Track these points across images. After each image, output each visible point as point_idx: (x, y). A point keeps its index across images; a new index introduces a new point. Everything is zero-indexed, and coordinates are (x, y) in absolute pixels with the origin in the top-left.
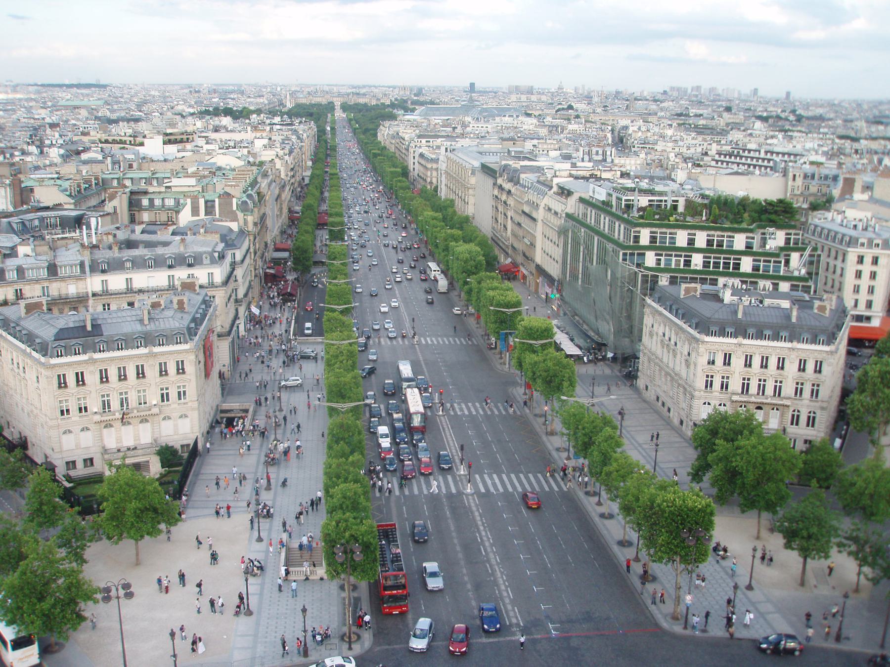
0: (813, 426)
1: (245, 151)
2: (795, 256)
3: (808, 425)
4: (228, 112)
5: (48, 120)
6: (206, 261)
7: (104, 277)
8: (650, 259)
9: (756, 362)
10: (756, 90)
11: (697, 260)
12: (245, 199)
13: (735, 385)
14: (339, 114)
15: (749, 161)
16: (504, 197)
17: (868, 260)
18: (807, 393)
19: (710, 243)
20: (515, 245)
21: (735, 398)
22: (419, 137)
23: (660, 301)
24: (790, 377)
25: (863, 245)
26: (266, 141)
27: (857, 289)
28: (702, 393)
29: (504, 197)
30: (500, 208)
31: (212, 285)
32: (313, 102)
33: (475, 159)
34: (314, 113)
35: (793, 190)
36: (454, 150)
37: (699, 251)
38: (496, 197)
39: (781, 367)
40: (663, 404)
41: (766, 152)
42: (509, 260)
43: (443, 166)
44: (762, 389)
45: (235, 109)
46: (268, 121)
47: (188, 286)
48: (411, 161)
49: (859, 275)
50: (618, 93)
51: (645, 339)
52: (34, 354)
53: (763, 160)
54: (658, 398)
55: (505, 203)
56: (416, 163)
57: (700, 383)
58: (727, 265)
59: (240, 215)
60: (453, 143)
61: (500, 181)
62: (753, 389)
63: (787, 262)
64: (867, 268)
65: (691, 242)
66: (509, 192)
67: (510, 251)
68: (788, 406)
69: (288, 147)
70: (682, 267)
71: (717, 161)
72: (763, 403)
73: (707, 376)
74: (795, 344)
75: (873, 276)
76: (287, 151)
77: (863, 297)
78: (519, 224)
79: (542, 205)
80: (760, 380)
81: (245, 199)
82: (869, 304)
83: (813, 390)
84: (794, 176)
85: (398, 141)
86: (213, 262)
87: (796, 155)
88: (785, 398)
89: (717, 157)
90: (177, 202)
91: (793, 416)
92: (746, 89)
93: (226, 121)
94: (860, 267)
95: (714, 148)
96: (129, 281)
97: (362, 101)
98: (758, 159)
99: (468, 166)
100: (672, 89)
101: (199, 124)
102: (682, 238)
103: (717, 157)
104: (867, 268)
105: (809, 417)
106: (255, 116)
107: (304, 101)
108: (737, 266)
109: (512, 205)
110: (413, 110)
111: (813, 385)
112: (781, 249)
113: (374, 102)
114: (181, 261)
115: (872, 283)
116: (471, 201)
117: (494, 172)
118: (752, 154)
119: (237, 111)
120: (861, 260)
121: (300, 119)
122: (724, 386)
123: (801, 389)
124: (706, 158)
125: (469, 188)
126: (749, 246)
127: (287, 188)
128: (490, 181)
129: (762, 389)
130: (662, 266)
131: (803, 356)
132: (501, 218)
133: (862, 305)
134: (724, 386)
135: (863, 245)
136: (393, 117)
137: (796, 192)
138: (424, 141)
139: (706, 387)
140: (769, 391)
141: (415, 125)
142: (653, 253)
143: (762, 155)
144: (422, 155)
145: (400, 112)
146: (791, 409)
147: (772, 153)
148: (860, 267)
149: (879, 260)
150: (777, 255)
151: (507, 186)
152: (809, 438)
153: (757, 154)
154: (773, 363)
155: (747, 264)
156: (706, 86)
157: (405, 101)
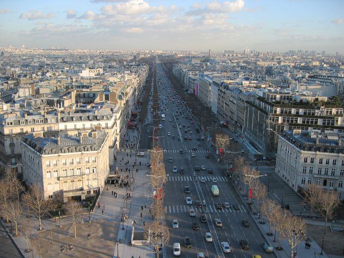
5: (45, 63)
6: (105, 118)
7: (65, 124)
12: (121, 94)
13: (315, 171)
15: (323, 80)
16: (222, 95)
19: (305, 113)
21: (315, 176)
23: (284, 136)
28: (302, 174)
31: (107, 128)
34: (148, 61)
35: (339, 92)
37: (300, 116)
38: (219, 94)
40: (286, 178)
46: (130, 64)
47: (98, 128)
51: (278, 152)
52: (38, 153)
54: (284, 176)
57: (301, 170)
58: (312, 122)
59: (119, 101)
62: (323, 173)
63: (337, 121)
65: (298, 113)
66: (224, 93)
68: (337, 179)
76: (137, 76)
80: (326, 169)
81: (121, 94)
86: (108, 119)
90: (94, 95)
95: (307, 75)
96: (75, 125)
102: (293, 111)
108: (316, 122)
114: (96, 118)
117: (219, 85)
122: (311, 171)
124: (304, 79)
134: (311, 171)
138: (191, 72)
139: (303, 171)
140: (330, 173)
143: (326, 78)
144: (190, 78)
151: (223, 90)
153: (325, 78)
155: (320, 122)
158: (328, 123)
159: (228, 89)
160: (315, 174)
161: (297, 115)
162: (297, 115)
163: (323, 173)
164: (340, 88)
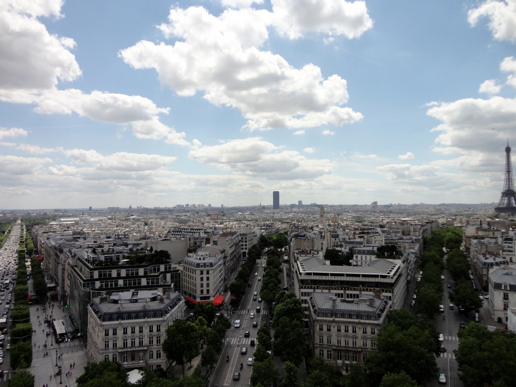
0: (160, 358)
2: (169, 276)
3: (157, 358)
8: (98, 284)
9: (129, 330)
10: (210, 205)
11: (121, 282)
13: (120, 344)
17: (205, 272)
18: (155, 342)
21: (120, 350)
23: (91, 306)
24: (146, 335)
25: (202, 266)
27: (202, 285)
35: (190, 245)
39: (141, 331)
41: (191, 229)
44: (133, 343)
49: (202, 279)
50: (155, 208)
53: (190, 232)
54: (92, 356)
62: (129, 345)
63: (165, 278)
64: (205, 276)
65: (119, 274)
70: (114, 287)
71: (172, 235)
72: (134, 351)
73: (106, 342)
74: (146, 319)
75: (208, 279)
77: (205, 289)
79: (67, 262)
80: (132, 339)
82: (208, 291)
83: (157, 340)
84: (190, 239)
87: (200, 230)
88: (145, 346)
89: (172, 233)
91: (150, 354)
92: (206, 205)
94: (202, 276)
98: (188, 232)
100: (177, 205)
102: (114, 273)
103: (172, 233)
104: (205, 276)
105: (157, 354)
108: (140, 283)
111: (157, 337)
112: (162, 273)
115: (208, 282)
118: (186, 231)
120: (202, 273)
122: (115, 345)
123: (152, 340)
124: (169, 234)
126: (145, 273)
129: (133, 343)
130: (104, 287)
131: (151, 324)
133: (205, 292)
134: (115, 345)
135: (202, 266)
137: (192, 245)
138: (45, 234)
142: (99, 282)
146: (149, 351)
147: (193, 229)
148: (202, 276)
149: (211, 272)
150: (158, 276)
152: (159, 364)
154: (137, 329)
155: (144, 282)
156: (191, 204)
157: (55, 216)
158: (153, 283)
160: (120, 349)
161: (119, 277)
162: (119, 277)
163: (129, 345)
164: (190, 240)
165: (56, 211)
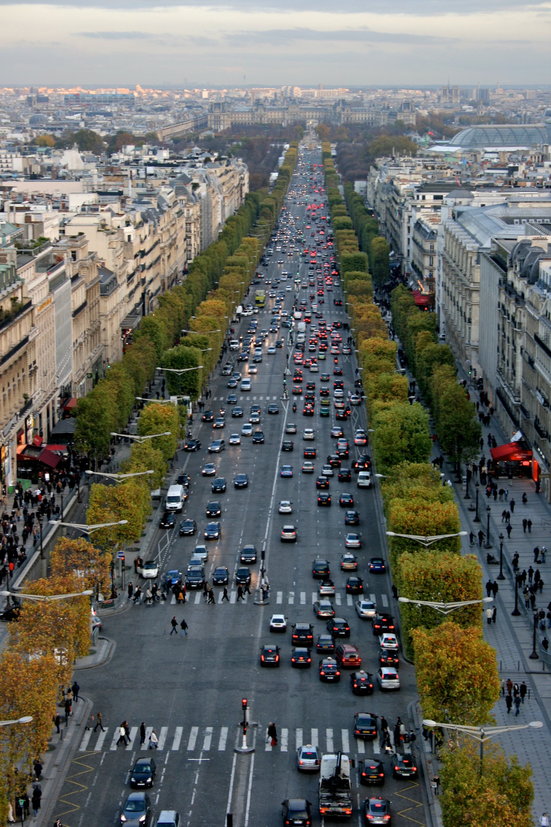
1: (20, 217)
4: (85, 141)
14: (309, 144)
20: (527, 407)
22: (424, 188)
26: (91, 198)
29: (512, 309)
30: (508, 333)
32: (265, 121)
33: (487, 232)
36: (460, 214)
38: (503, 307)
42: (518, 436)
43: (439, 245)
45: (103, 134)
46: (146, 158)
48: (405, 236)
55: (513, 319)
56: (412, 242)
60: (465, 201)
61: (511, 276)
66: (520, 299)
67: (520, 417)
69: (143, 209)
78: (531, 362)
85: (391, 195)
93: (71, 158)
97: (359, 117)
99: (471, 246)
101: (18, 163)
106: (130, 148)
107: (246, 119)
109: (524, 325)
110: (450, 135)
113: (384, 120)
116: (476, 314)
119: (106, 138)
121: (207, 154)
125: (471, 291)
127: (123, 291)
128: (497, 276)
132: (509, 347)
136: (411, 150)
138: (429, 197)
141: (434, 163)
144: (418, 225)
145: (423, 140)
151: (520, 285)
159: (532, 276)
165: (448, 91)
